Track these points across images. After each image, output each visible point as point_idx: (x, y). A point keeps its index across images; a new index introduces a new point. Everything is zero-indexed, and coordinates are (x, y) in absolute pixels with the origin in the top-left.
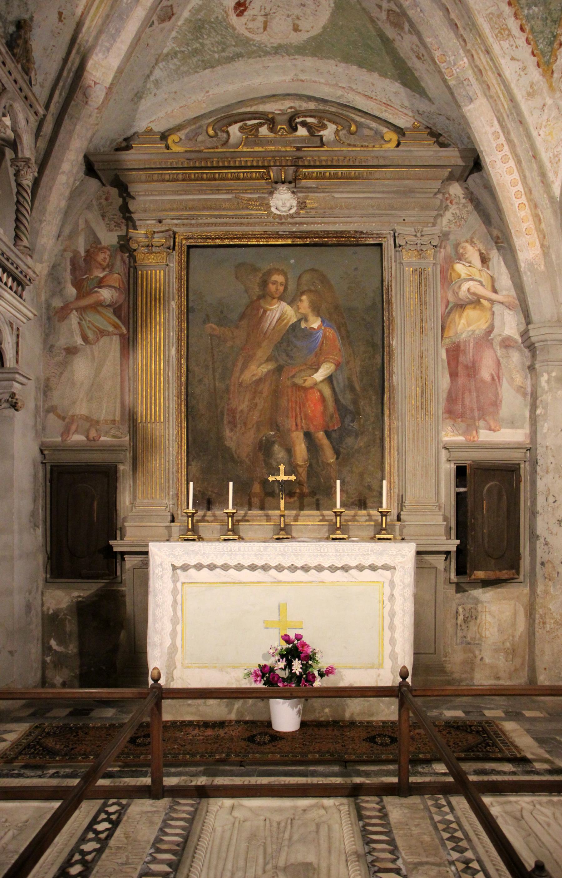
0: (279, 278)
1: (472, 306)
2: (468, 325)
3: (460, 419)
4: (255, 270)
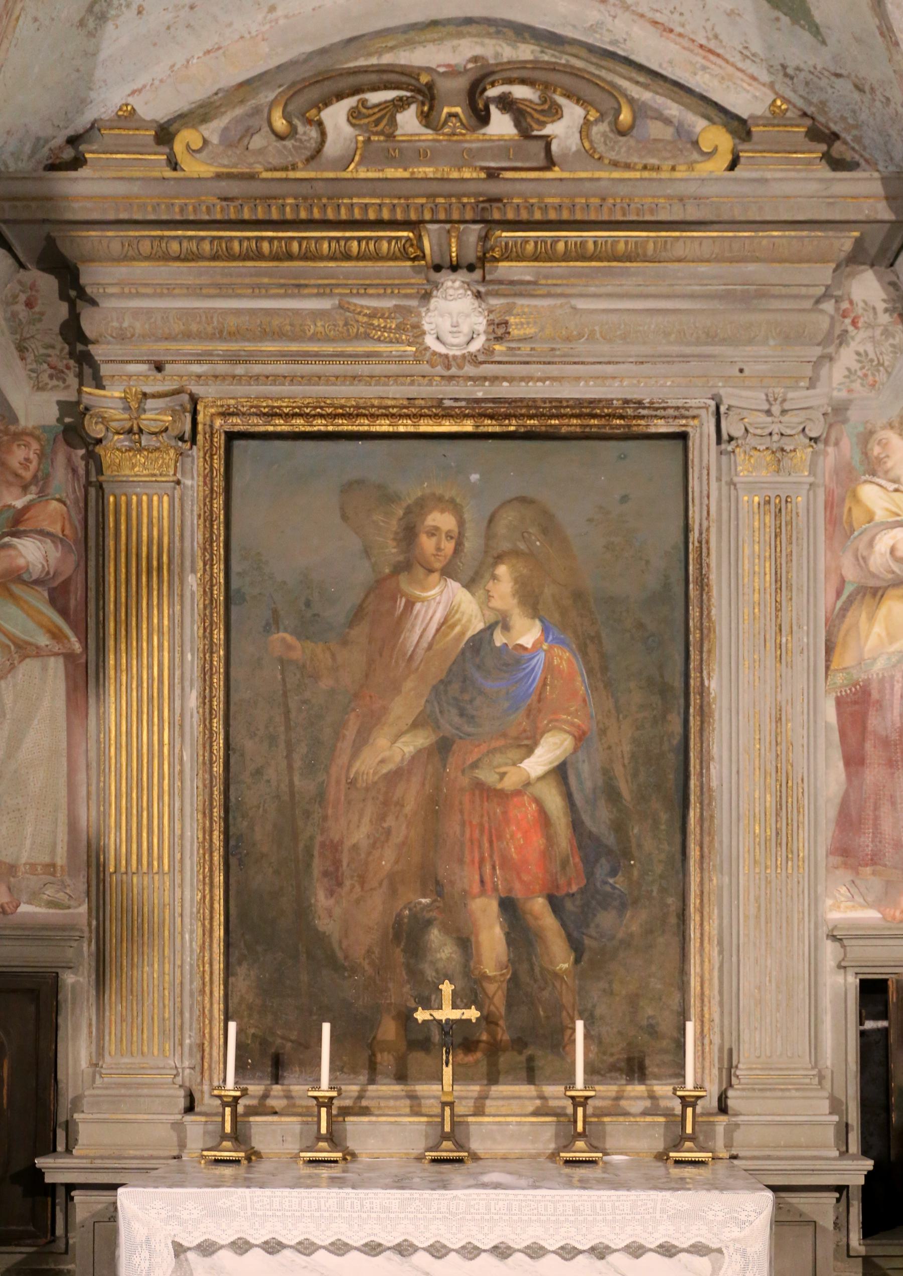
0: (443, 520)
4: (388, 498)
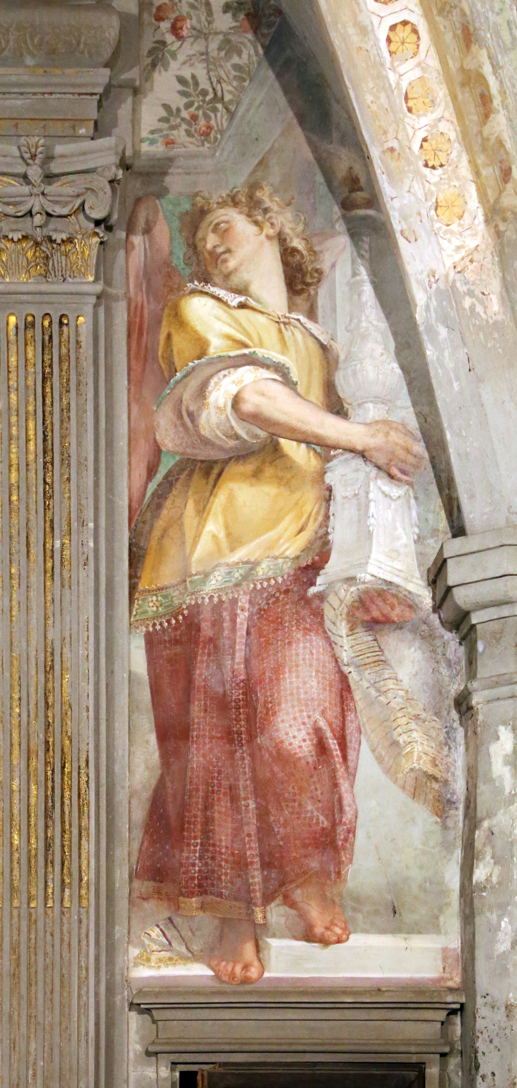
1: (249, 467)
2: (230, 542)
3: (194, 901)
